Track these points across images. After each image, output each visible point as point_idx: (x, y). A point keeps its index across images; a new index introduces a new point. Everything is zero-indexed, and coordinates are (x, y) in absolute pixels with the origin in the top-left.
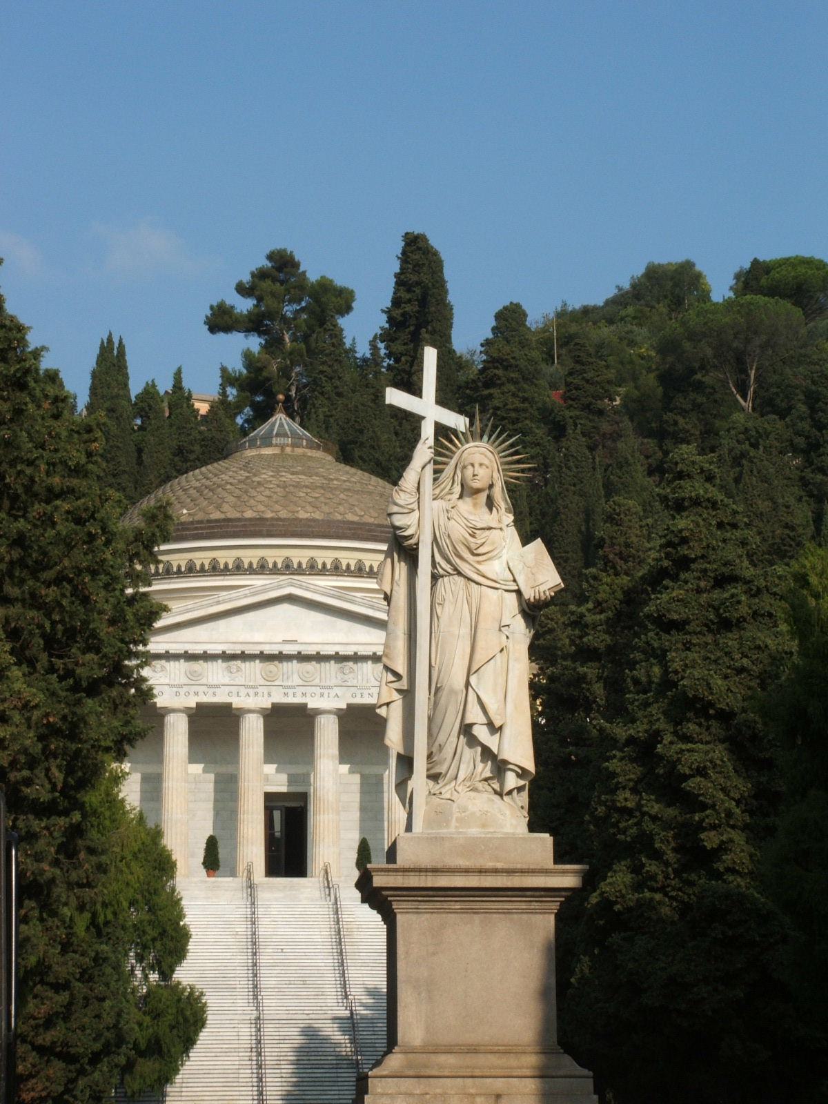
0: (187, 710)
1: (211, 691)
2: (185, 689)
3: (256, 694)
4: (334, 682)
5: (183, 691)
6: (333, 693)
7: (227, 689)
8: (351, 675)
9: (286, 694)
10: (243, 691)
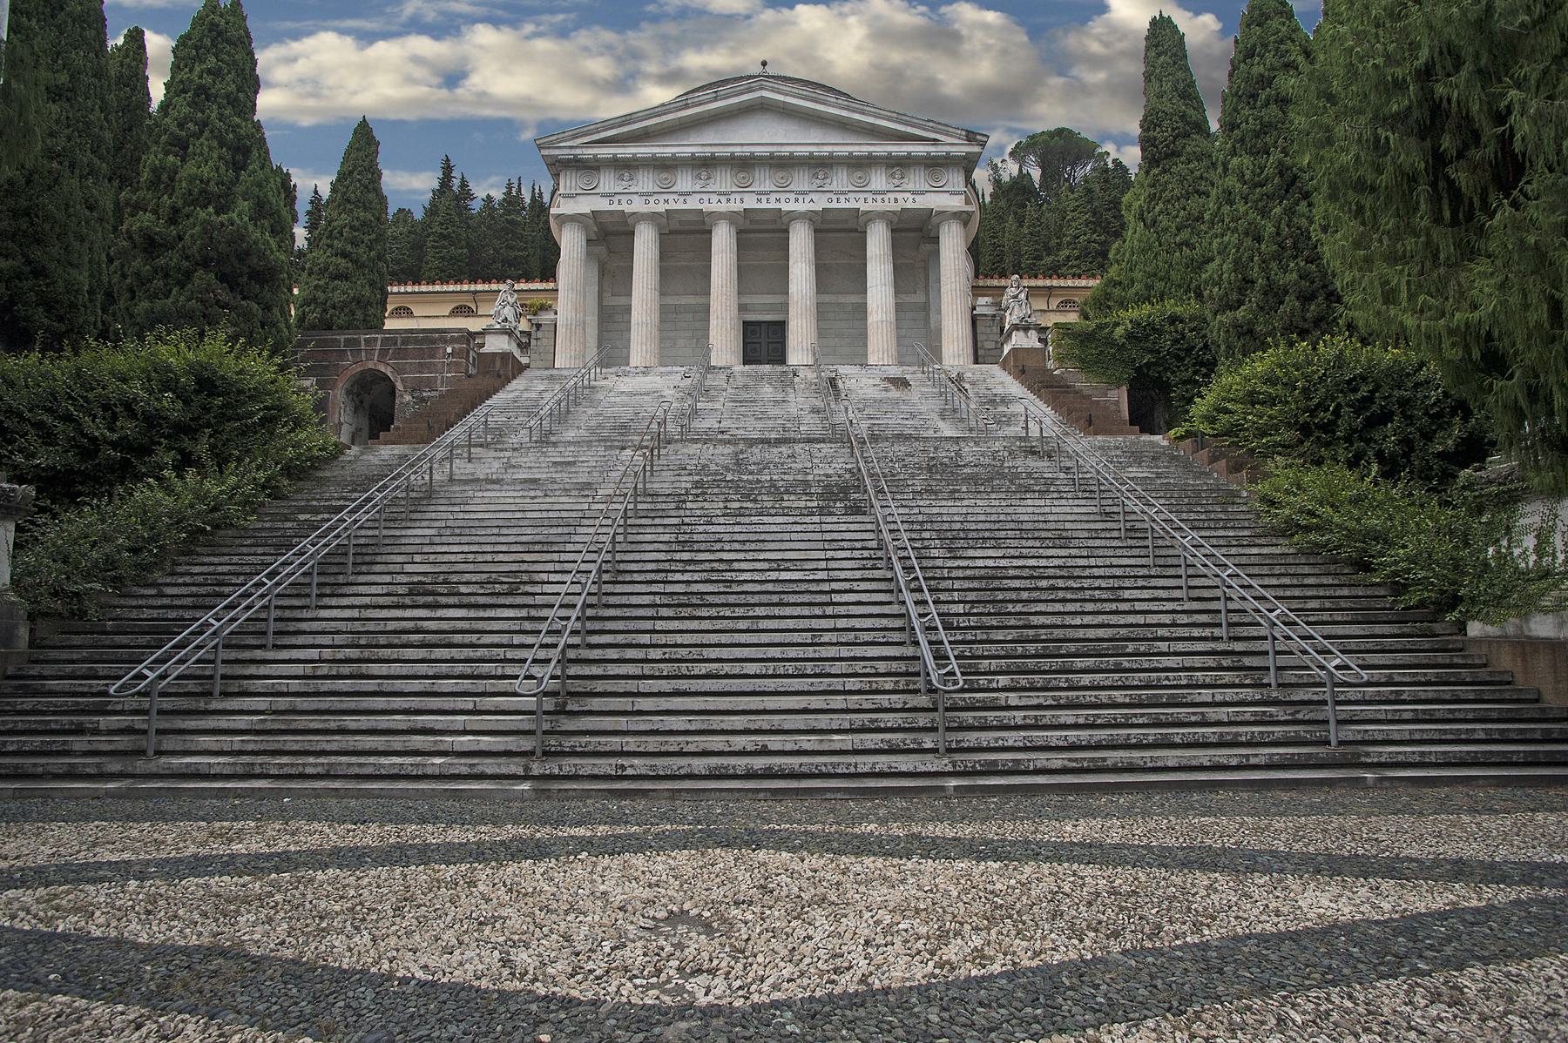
5: (651, 199)
6: (807, 199)
7: (698, 196)
9: (759, 201)
10: (715, 198)
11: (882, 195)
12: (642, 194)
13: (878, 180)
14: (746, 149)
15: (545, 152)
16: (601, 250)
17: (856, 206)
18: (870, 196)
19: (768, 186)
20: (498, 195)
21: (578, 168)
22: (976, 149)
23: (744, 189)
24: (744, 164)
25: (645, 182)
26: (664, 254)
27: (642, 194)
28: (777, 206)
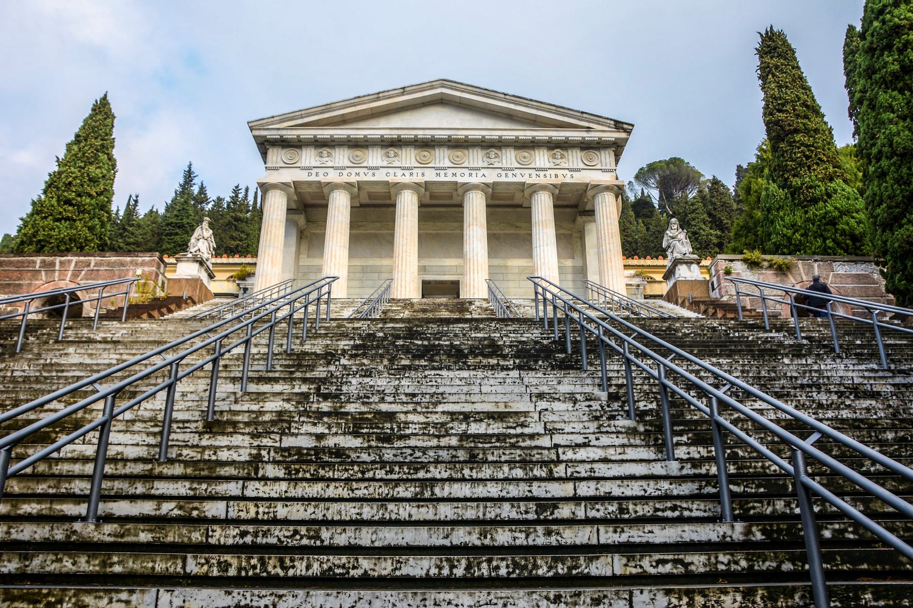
1: (371, 172)
2: (348, 170)
4: (481, 164)
5: (345, 172)
6: (480, 173)
8: (497, 160)
10: (399, 172)
11: (544, 171)
13: (542, 158)
14: (427, 132)
15: (257, 133)
16: (301, 220)
17: (522, 180)
18: (533, 172)
19: (447, 163)
20: (227, 197)
21: (283, 147)
22: (623, 135)
23: (423, 165)
24: (426, 144)
25: (341, 157)
26: (355, 223)
28: (454, 179)
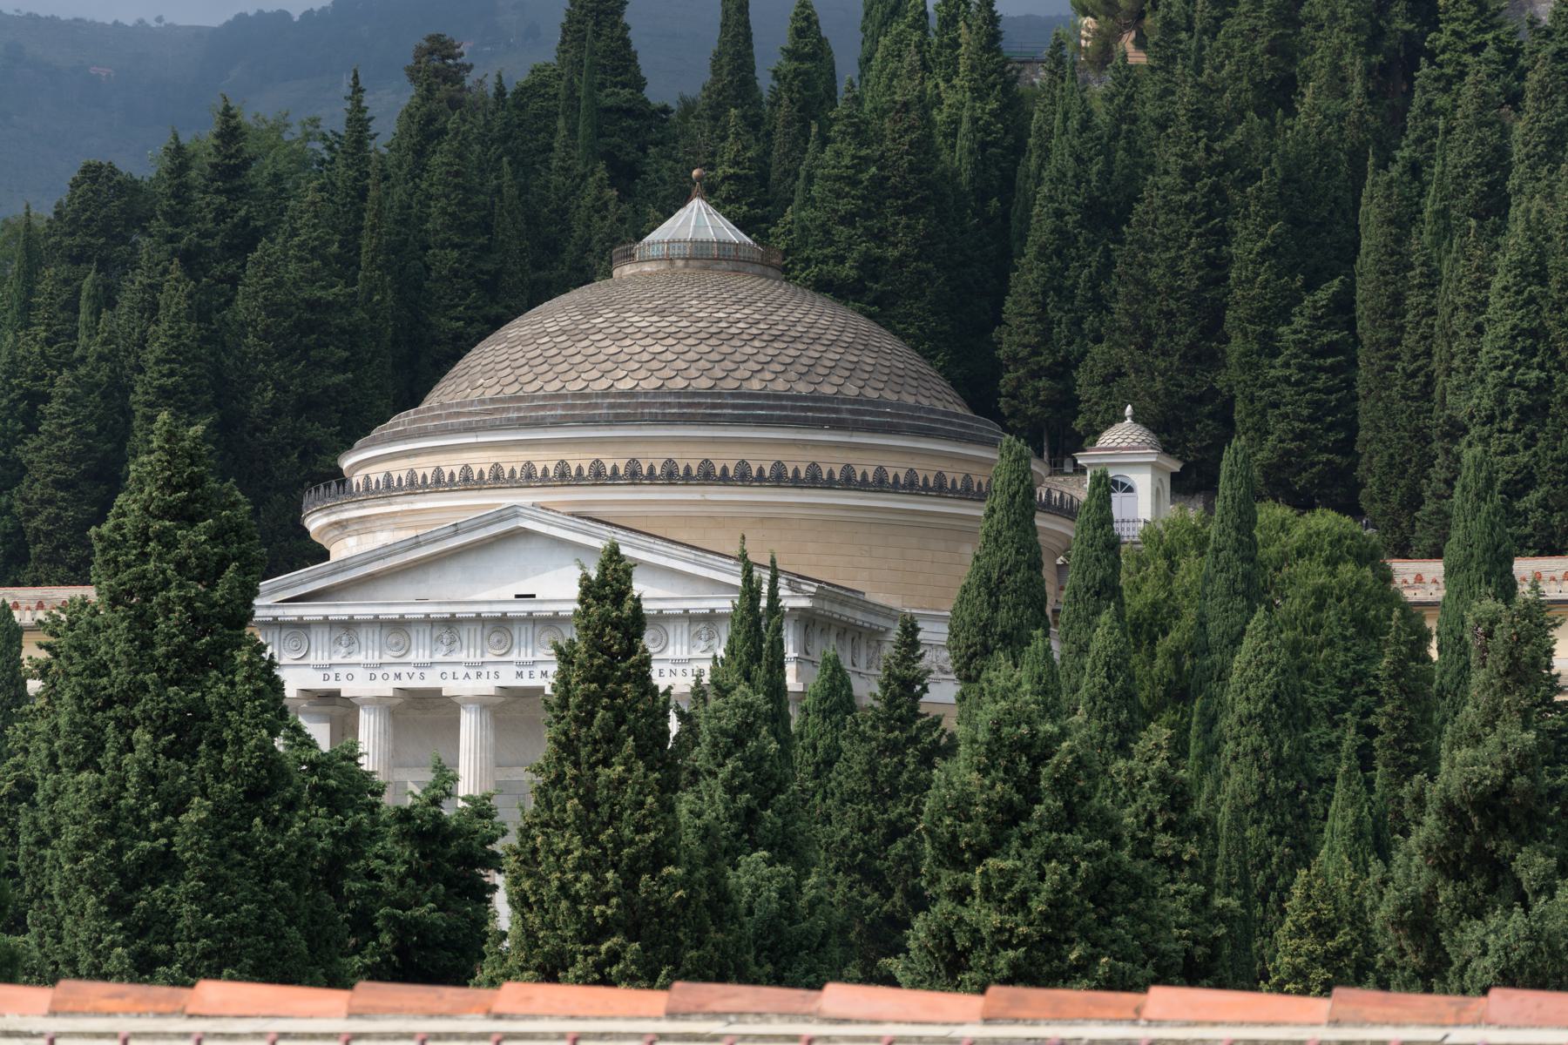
0: (378, 701)
1: (418, 672)
3: (479, 675)
5: (379, 673)
7: (439, 669)
9: (520, 675)
10: (461, 671)
12: (366, 666)
27: (366, 666)
